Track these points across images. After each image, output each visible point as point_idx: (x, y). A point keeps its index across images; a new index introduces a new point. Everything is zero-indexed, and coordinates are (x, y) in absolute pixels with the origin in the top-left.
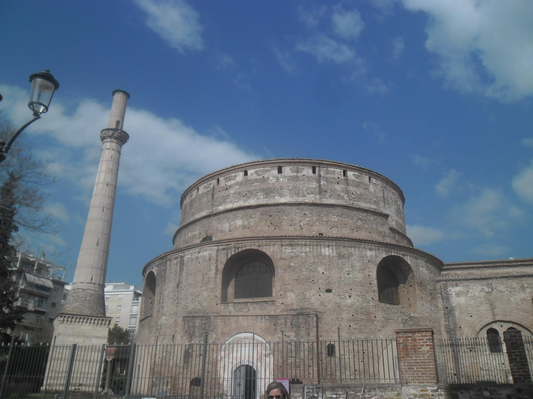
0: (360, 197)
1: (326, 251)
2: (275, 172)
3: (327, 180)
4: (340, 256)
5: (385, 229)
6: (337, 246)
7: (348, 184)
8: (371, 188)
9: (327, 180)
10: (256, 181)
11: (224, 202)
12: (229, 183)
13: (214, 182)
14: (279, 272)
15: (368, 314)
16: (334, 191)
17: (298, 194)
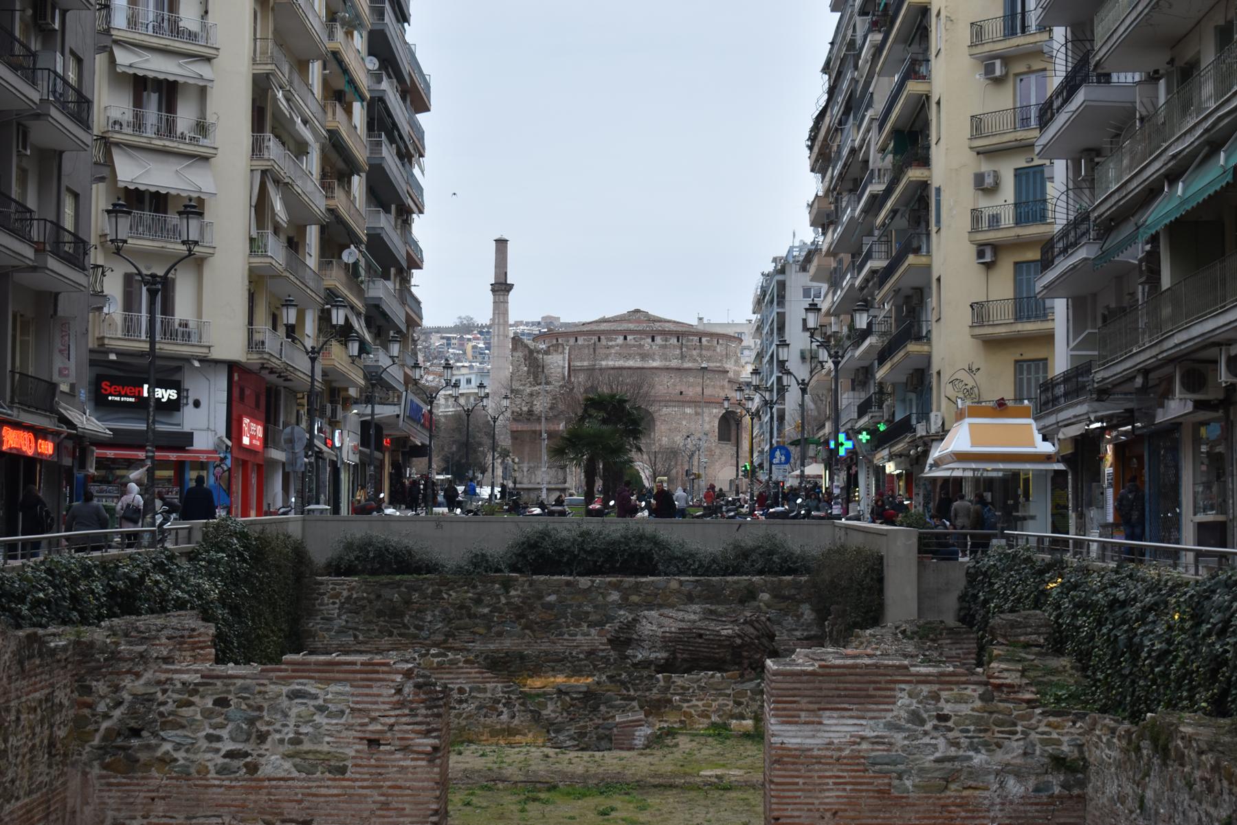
0: (709, 360)
1: (688, 410)
2: (650, 340)
3: (687, 347)
4: (697, 414)
5: (726, 383)
6: (695, 407)
7: (701, 349)
8: (718, 350)
9: (687, 347)
10: (634, 346)
11: (607, 357)
12: (610, 344)
13: (595, 338)
14: (658, 423)
15: (711, 451)
16: (691, 356)
17: (666, 359)
